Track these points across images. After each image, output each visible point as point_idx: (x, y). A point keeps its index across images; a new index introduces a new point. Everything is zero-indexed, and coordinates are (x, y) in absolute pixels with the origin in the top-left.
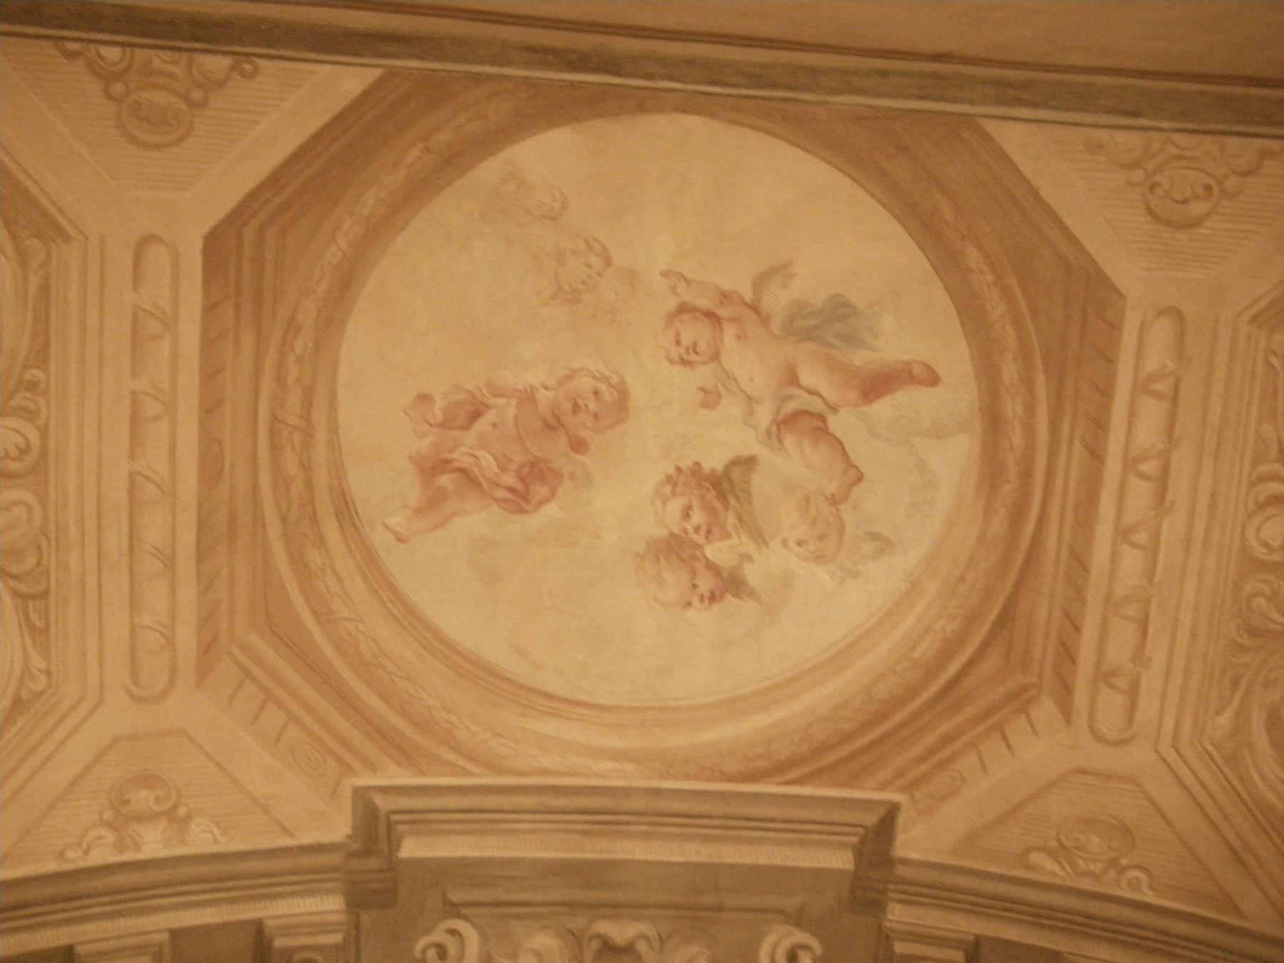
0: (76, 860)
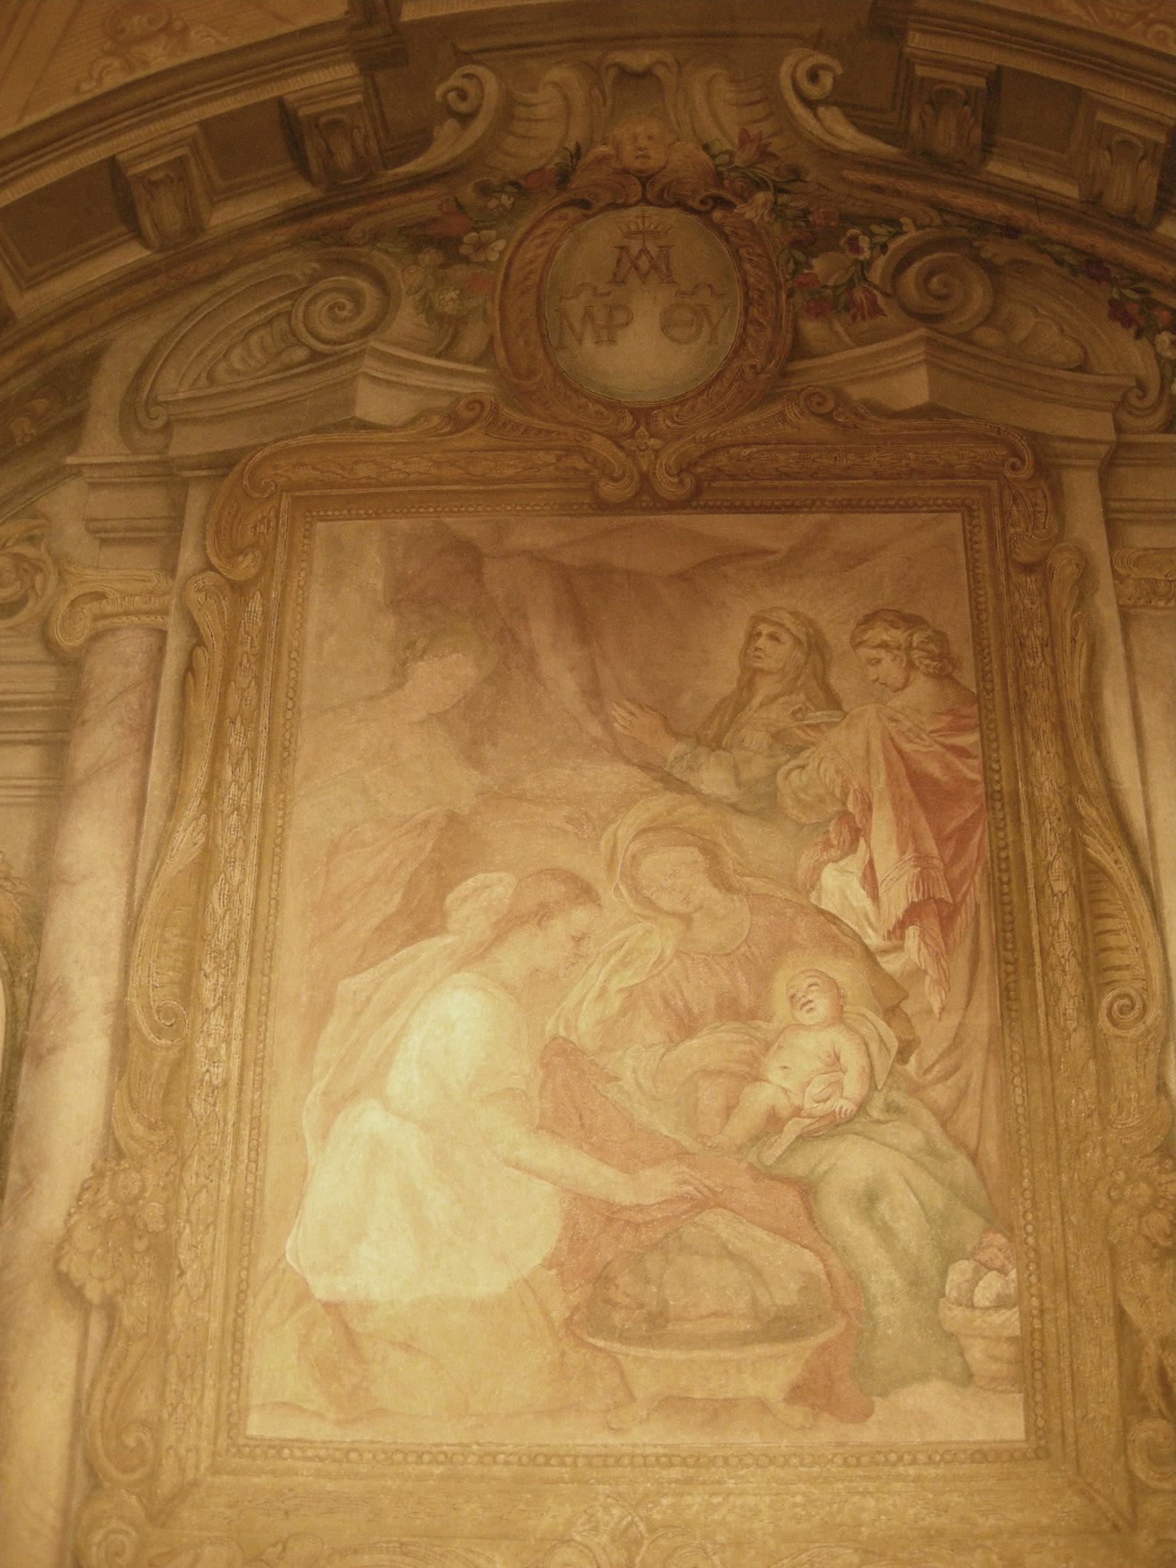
0: (90, 90)
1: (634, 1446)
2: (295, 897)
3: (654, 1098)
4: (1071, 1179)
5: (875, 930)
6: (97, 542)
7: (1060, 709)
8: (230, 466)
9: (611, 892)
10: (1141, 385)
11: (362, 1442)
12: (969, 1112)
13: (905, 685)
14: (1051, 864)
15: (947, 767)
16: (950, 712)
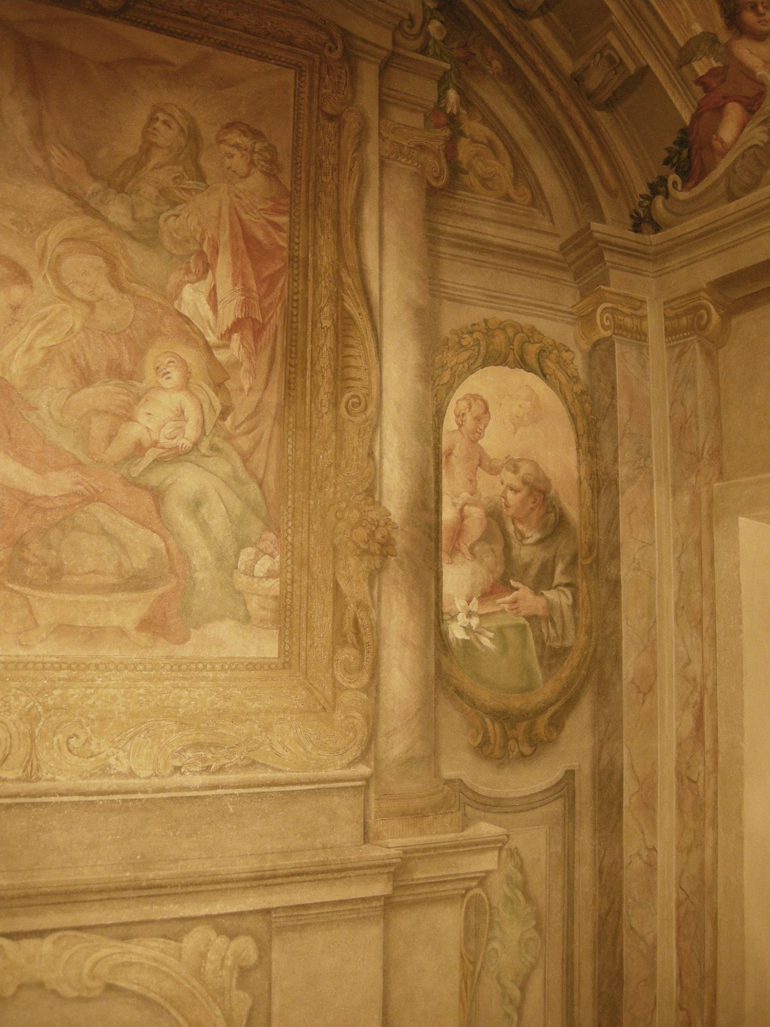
1: (37, 656)
3: (61, 425)
4: (315, 504)
5: (213, 332)
7: (338, 212)
10: (411, 19)
12: (259, 457)
13: (248, 175)
14: (322, 308)
15: (268, 234)
16: (273, 199)
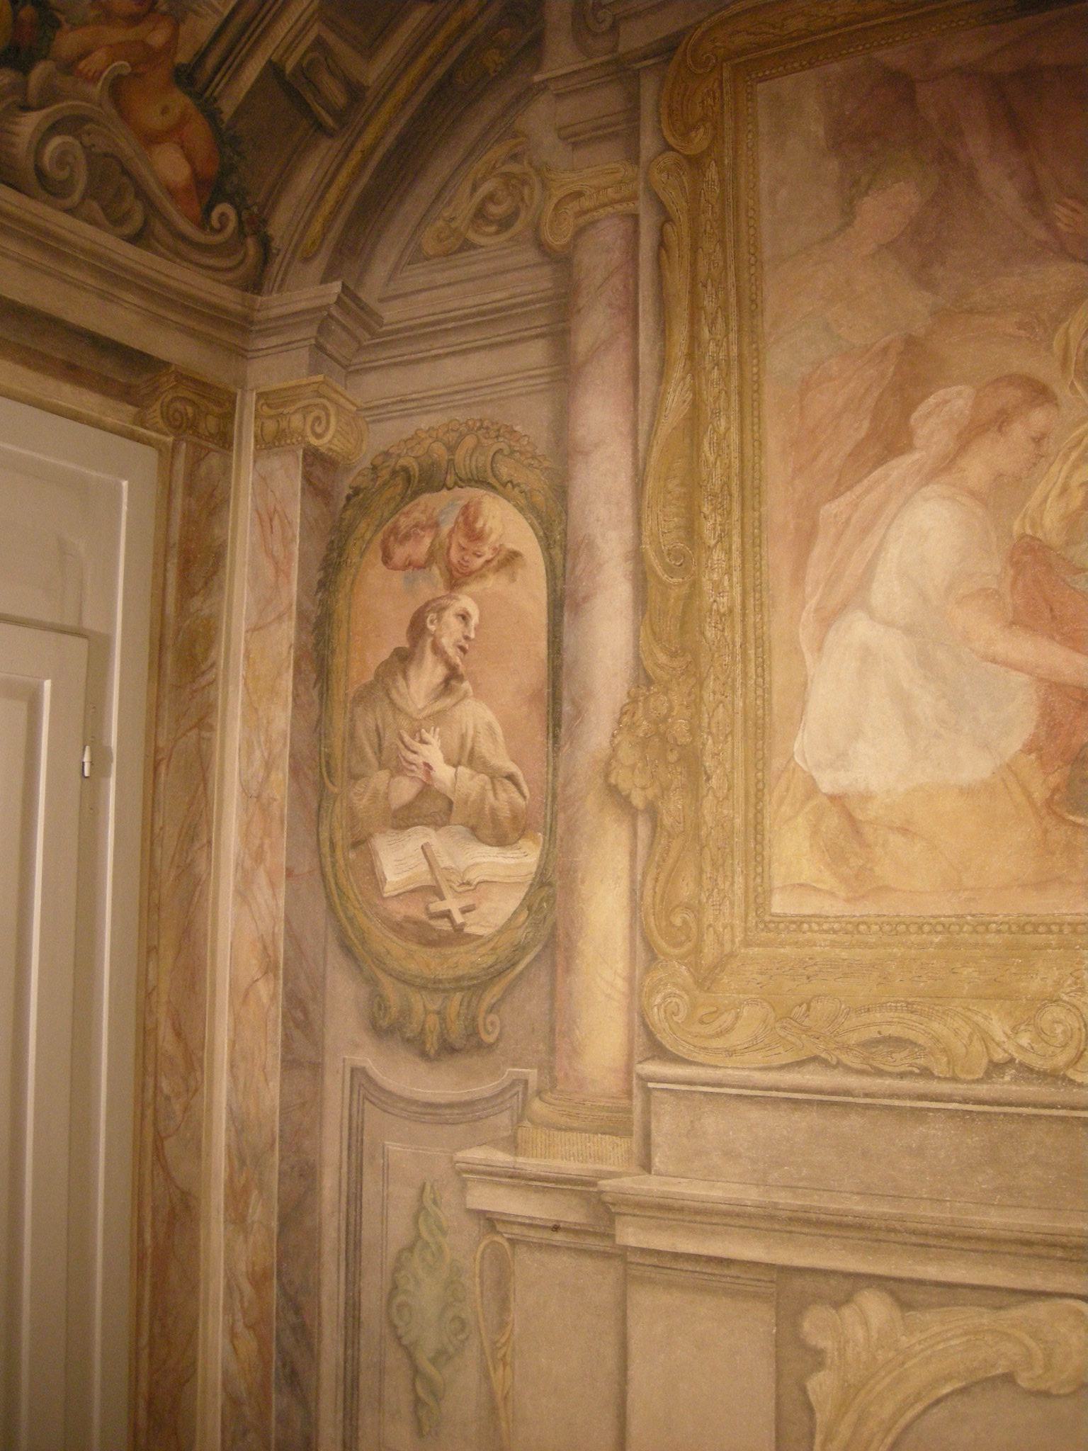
2: (775, 435)
6: (570, 148)
8: (673, 49)
9: (1067, 391)
11: (868, 916)
